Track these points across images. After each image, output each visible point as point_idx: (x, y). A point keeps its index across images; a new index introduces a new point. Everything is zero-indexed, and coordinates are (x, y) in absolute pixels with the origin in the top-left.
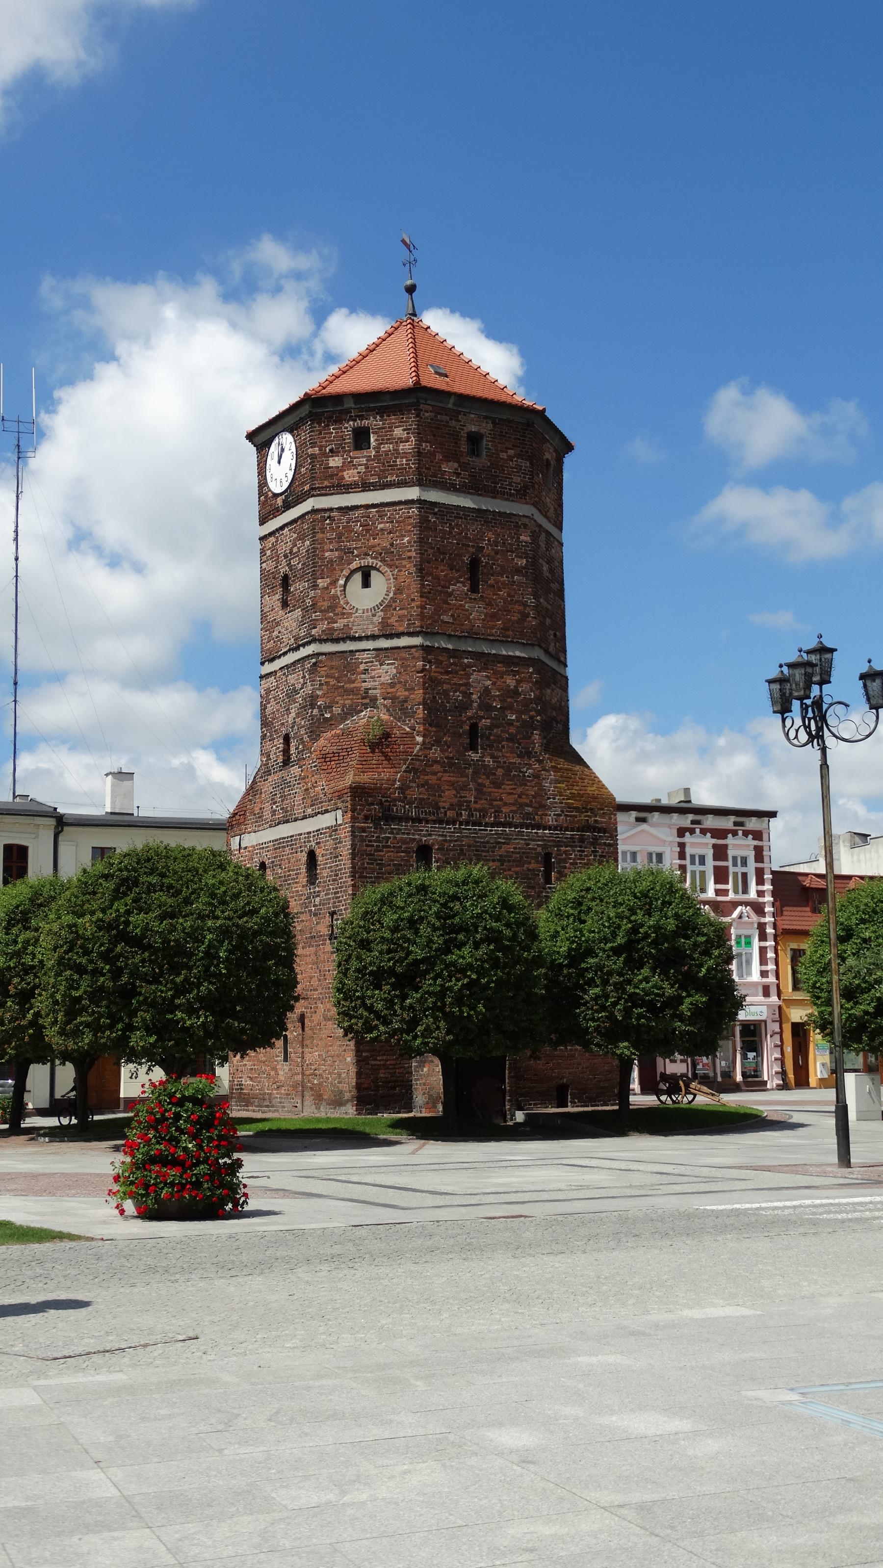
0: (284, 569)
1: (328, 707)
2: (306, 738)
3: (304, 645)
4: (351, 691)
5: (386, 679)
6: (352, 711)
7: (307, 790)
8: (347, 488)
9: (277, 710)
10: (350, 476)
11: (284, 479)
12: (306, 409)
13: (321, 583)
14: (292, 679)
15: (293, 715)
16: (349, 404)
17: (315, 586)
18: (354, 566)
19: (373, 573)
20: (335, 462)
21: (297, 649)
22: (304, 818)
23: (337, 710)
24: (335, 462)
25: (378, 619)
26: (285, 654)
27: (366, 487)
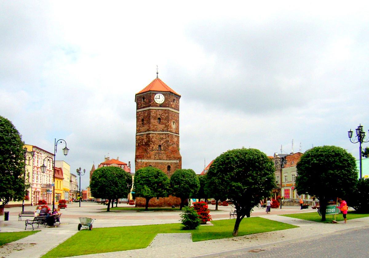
0: (159, 116)
1: (170, 143)
2: (167, 147)
3: (165, 131)
4: (172, 141)
5: (176, 140)
6: (172, 144)
7: (167, 156)
8: (172, 108)
9: (157, 140)
10: (173, 106)
11: (160, 102)
12: (169, 93)
13: (170, 122)
14: (162, 136)
15: (162, 142)
16: (174, 95)
17: (169, 122)
18: (173, 121)
19: (174, 123)
20: (172, 103)
21: (163, 131)
22: (167, 160)
23: (171, 144)
24: (172, 103)
25: (175, 130)
26: (159, 131)
27: (174, 109)
